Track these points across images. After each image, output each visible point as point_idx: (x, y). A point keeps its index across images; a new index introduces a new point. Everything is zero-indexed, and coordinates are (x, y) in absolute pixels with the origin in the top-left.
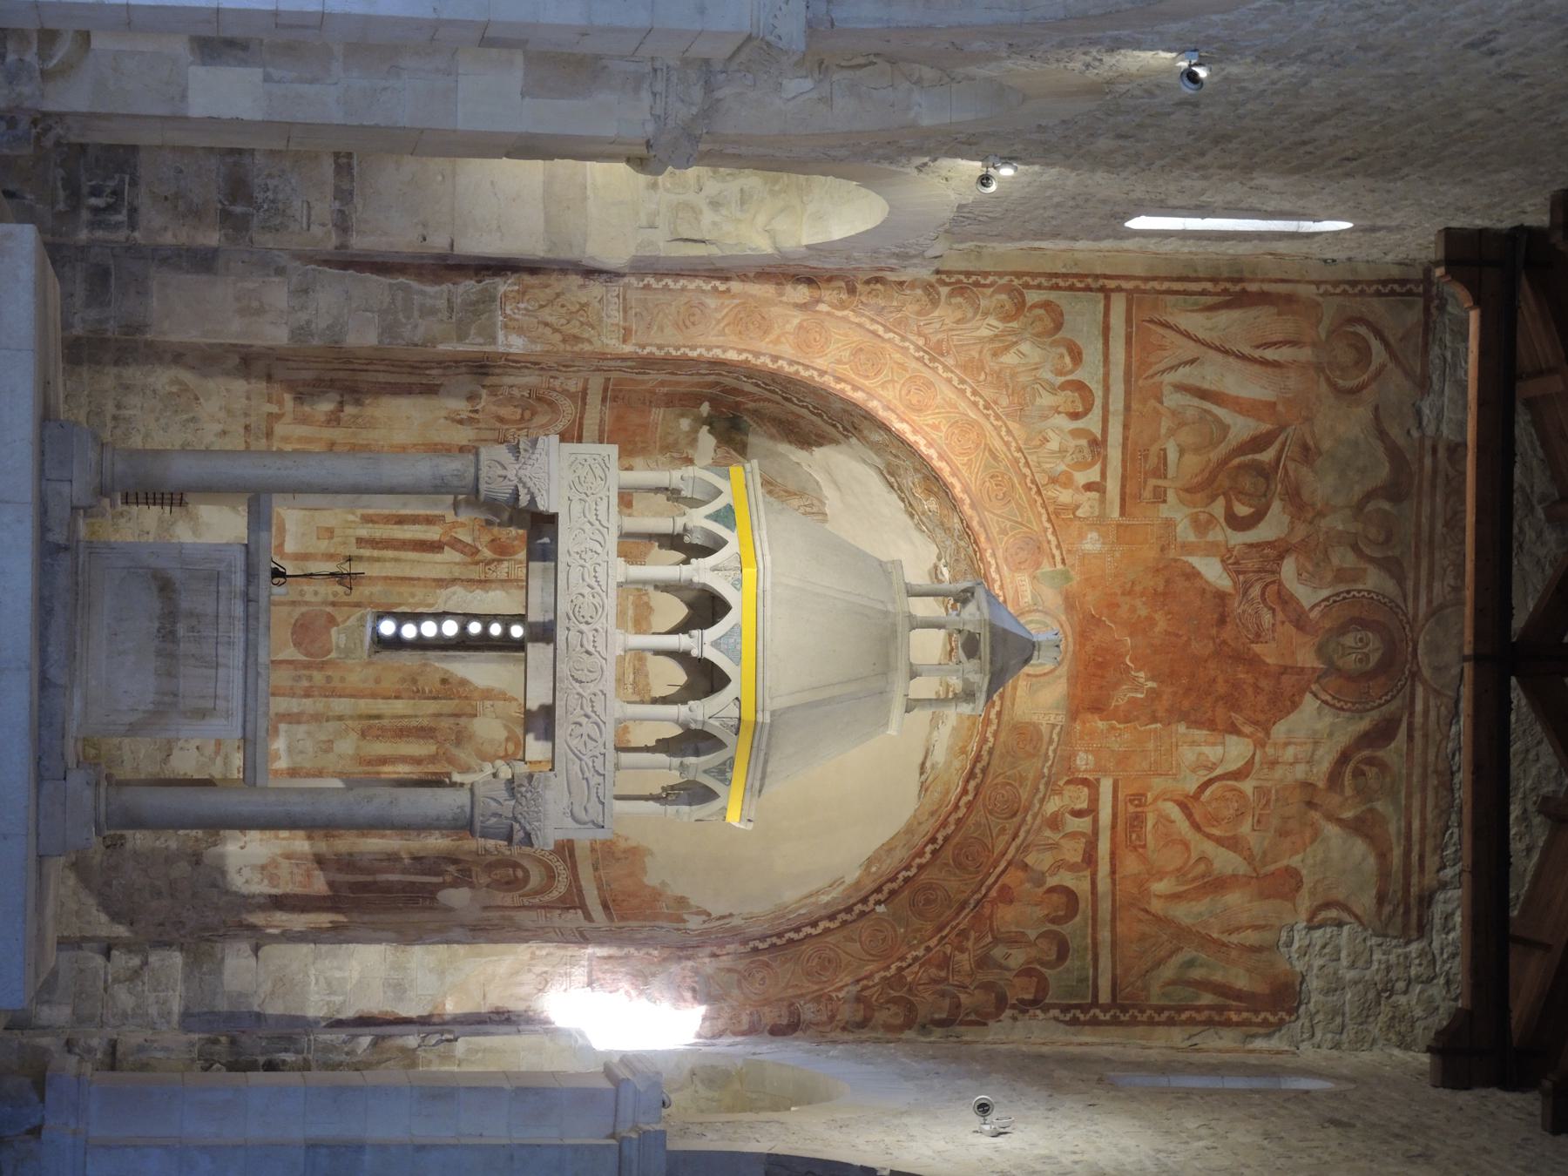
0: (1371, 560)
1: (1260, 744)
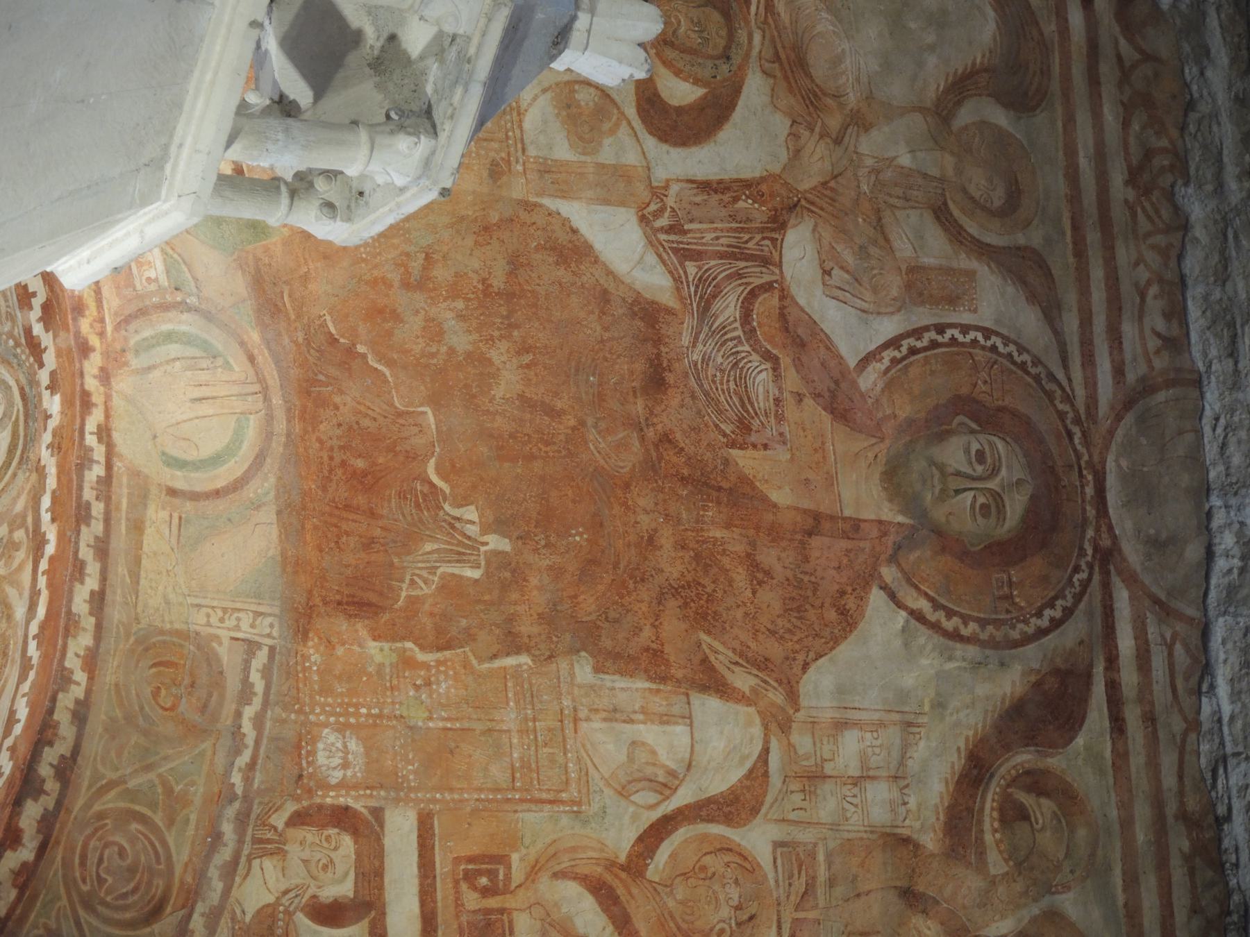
0: (983, 250)
1: (778, 723)
